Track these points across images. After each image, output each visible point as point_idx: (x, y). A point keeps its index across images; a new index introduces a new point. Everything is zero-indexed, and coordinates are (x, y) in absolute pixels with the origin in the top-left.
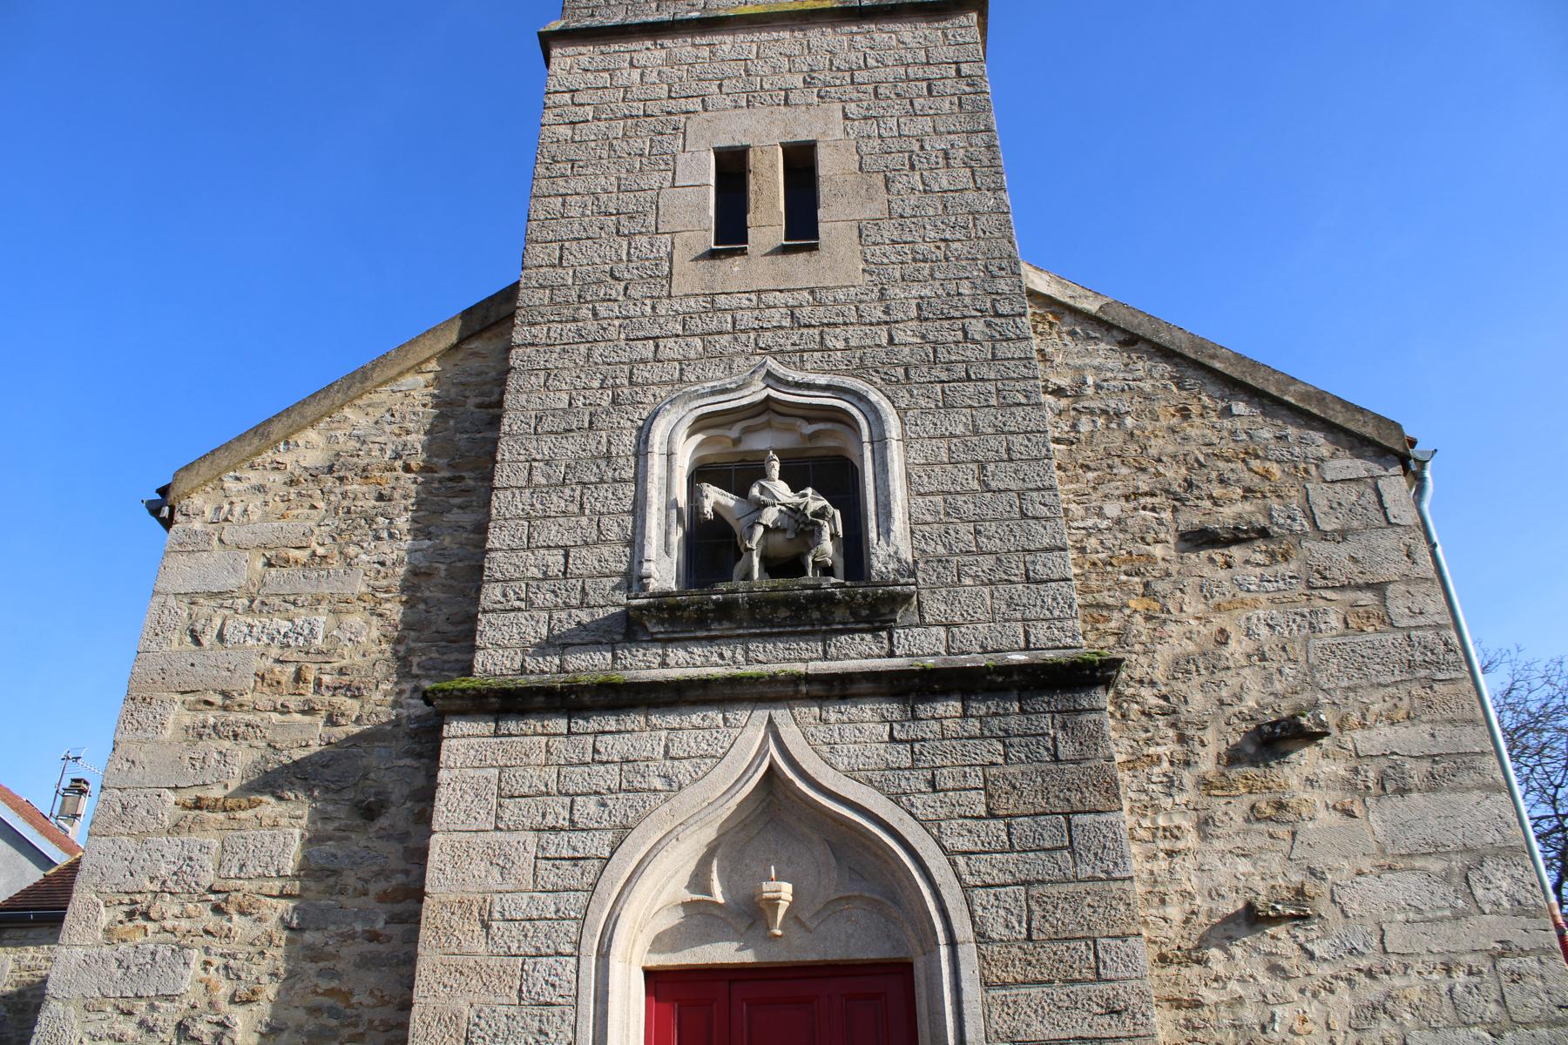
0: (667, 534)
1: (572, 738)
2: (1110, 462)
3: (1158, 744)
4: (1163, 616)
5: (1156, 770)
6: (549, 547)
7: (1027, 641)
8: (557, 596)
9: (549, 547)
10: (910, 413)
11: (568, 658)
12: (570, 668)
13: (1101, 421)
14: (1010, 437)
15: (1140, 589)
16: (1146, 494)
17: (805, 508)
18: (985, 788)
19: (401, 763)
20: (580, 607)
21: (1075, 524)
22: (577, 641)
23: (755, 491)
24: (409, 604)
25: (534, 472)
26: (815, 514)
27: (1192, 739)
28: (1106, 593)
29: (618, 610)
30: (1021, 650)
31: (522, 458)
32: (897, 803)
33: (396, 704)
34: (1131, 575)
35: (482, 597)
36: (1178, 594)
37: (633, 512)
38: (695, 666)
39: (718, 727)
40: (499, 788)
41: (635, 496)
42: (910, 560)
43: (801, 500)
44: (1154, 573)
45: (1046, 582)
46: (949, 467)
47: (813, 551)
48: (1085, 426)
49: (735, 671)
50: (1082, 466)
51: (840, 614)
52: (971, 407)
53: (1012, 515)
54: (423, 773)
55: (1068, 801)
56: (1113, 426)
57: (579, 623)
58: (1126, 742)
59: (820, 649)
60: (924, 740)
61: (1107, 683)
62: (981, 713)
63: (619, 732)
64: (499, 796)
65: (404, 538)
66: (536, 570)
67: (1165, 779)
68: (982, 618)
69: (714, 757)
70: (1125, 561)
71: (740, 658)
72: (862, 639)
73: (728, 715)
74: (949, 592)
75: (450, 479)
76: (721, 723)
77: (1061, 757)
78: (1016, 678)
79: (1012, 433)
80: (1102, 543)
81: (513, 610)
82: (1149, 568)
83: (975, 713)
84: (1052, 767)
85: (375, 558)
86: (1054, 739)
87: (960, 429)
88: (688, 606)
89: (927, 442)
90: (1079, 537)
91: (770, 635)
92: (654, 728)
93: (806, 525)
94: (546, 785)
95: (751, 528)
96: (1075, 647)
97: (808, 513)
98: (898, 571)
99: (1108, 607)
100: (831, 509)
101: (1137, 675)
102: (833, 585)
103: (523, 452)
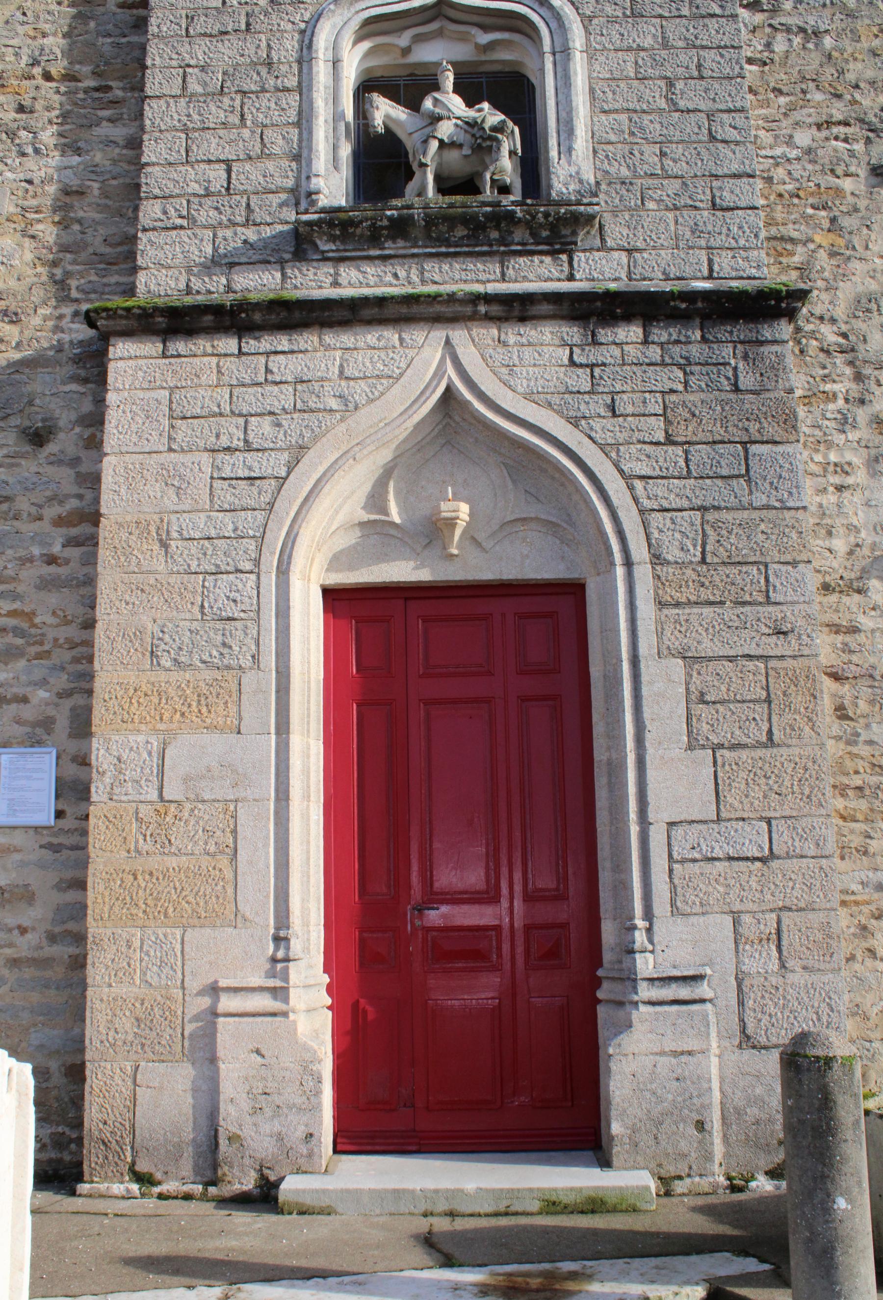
0: (335, 148)
1: (244, 358)
2: (804, 86)
3: (834, 381)
4: (848, 253)
5: (831, 406)
6: (209, 161)
7: (711, 270)
8: (221, 213)
9: (209, 161)
10: (595, 21)
11: (235, 277)
12: (238, 287)
13: (797, 40)
14: (701, 53)
15: (826, 224)
16: (839, 123)
17: (483, 121)
18: (664, 415)
19: (67, 388)
20: (246, 224)
21: (763, 153)
22: (244, 259)
23: (428, 104)
24: (64, 224)
25: (189, 79)
26: (494, 129)
27: (869, 378)
28: (791, 226)
29: (286, 228)
30: (704, 278)
31: (174, 63)
32: (576, 426)
33: (57, 329)
34: (818, 209)
35: (141, 214)
36: (865, 231)
37: (298, 124)
38: (368, 286)
39: (394, 347)
40: (170, 409)
41: (300, 106)
42: (592, 181)
43: (477, 115)
44: (841, 208)
45: (732, 209)
46: (636, 83)
47: (492, 168)
48: (780, 45)
49: (409, 290)
50: (774, 90)
51: (519, 234)
52: (661, 16)
53: (700, 137)
54: (91, 398)
55: (747, 430)
56: (810, 46)
57: (245, 242)
58: (803, 377)
59: (498, 271)
60: (604, 364)
61: (791, 315)
62: (663, 339)
63: (292, 352)
64: (171, 417)
65: (51, 154)
66: (196, 186)
67: (839, 416)
68: (665, 244)
69: (390, 377)
70: (812, 194)
71: (415, 278)
72: (542, 262)
73: (404, 335)
74: (632, 216)
75: (97, 89)
76: (397, 344)
77: (742, 387)
78: (700, 305)
79: (704, 47)
80: (790, 173)
81: (175, 228)
82: (837, 203)
83: (656, 339)
84: (732, 396)
85: (22, 176)
86: (735, 369)
87: (648, 42)
88: (361, 222)
89: (612, 54)
90: (766, 166)
91: (447, 255)
92: (328, 348)
93: (484, 139)
94: (219, 406)
95: (425, 142)
96: (759, 278)
97: (487, 126)
98: (579, 192)
99: (792, 240)
100: (510, 124)
101: (818, 311)
102: (513, 203)
103: (175, 56)
